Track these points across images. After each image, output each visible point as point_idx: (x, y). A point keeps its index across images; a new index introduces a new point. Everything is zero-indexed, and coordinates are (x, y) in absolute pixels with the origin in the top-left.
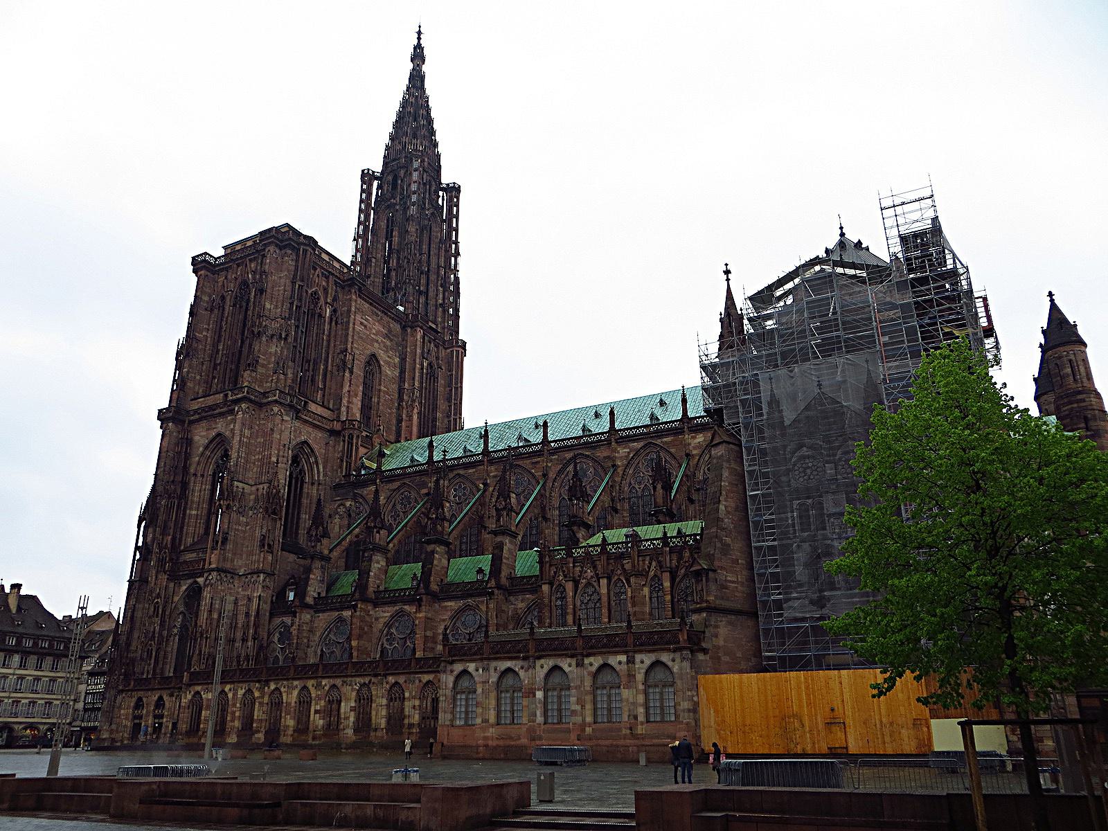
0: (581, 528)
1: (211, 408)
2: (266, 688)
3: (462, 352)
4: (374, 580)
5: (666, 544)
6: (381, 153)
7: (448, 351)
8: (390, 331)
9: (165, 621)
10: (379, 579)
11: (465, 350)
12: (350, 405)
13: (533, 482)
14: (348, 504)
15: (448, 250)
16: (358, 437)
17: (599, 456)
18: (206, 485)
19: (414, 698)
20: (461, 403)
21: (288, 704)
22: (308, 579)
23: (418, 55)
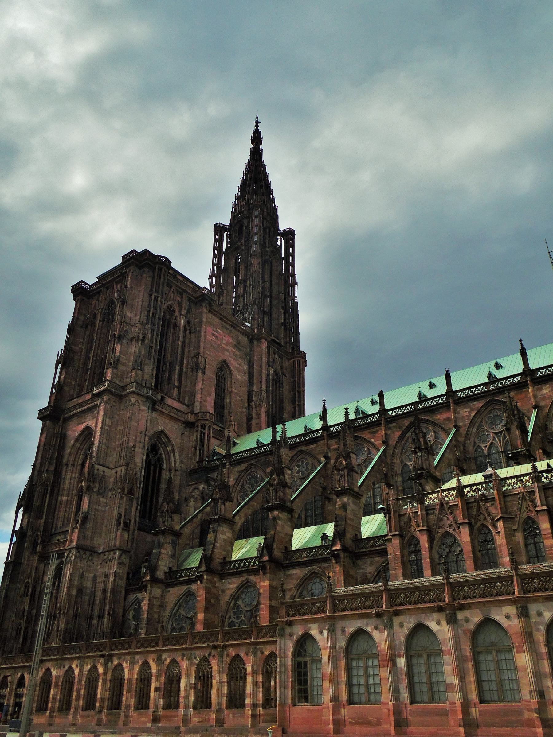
0: (429, 481)
2: (110, 663)
3: (303, 362)
4: (219, 551)
6: (230, 209)
7: (291, 361)
8: (239, 343)
9: (34, 601)
10: (224, 550)
11: (306, 361)
12: (204, 403)
14: (201, 487)
15: (287, 281)
16: (210, 427)
17: (439, 419)
20: (304, 405)
21: (130, 680)
23: (257, 138)
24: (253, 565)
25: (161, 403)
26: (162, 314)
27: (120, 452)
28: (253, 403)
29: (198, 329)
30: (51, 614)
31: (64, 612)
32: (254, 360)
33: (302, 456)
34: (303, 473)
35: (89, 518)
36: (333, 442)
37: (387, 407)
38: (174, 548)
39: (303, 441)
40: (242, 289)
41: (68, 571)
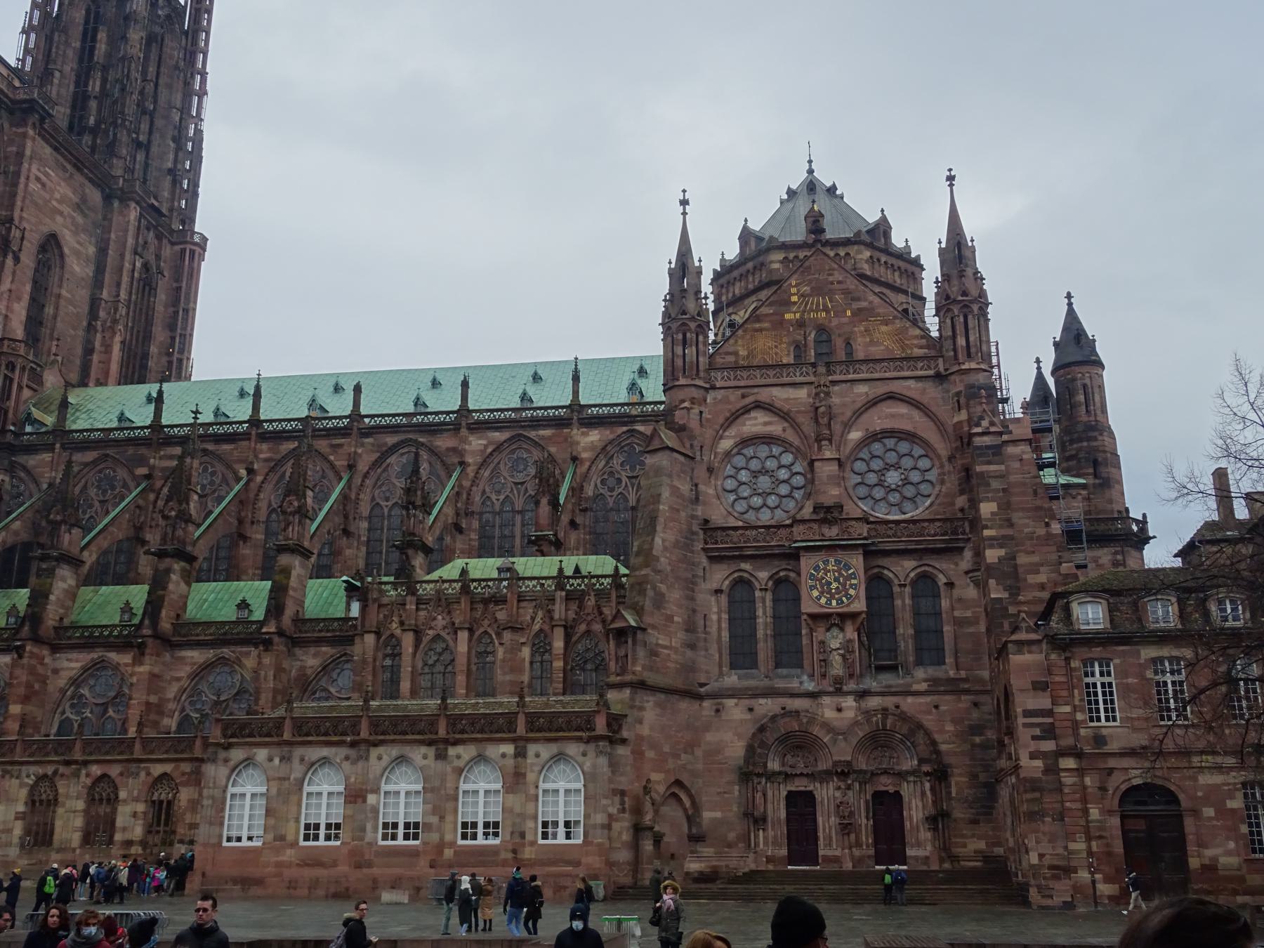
3: (200, 254)
4: (54, 607)
5: (560, 587)
7: (178, 248)
8: (84, 199)
10: (63, 606)
11: (205, 250)
13: (330, 474)
15: (188, 84)
16: (23, 369)
17: (437, 447)
19: (136, 800)
24: (116, 637)
28: (99, 323)
29: (12, 168)
32: (109, 239)
36: (264, 446)
37: (363, 411)
39: (210, 435)
40: (98, 83)
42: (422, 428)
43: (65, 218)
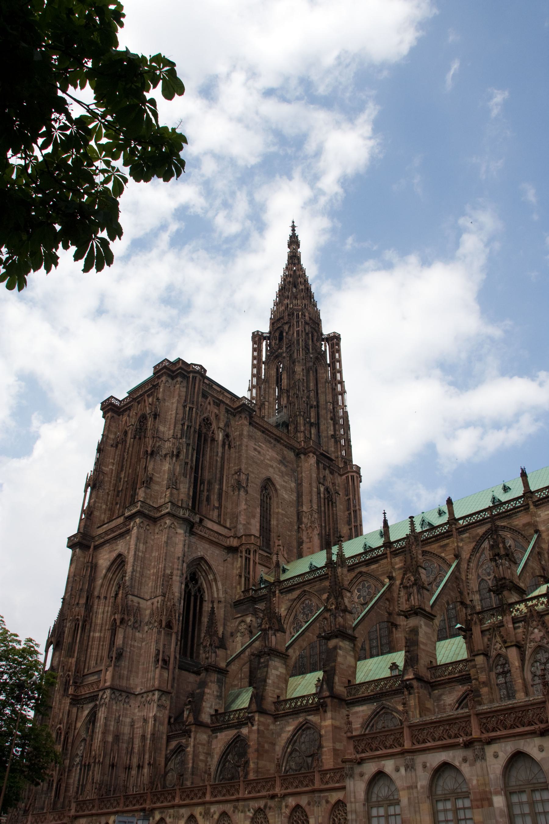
1: (112, 530)
3: (357, 477)
4: (272, 688)
7: (344, 477)
8: (284, 458)
9: (67, 749)
10: (278, 688)
11: (360, 476)
12: (249, 526)
13: (445, 567)
15: (334, 389)
16: (255, 551)
17: (517, 525)
18: (109, 606)
20: (361, 525)
22: (203, 694)
24: (312, 703)
25: (199, 526)
26: (197, 428)
27: (156, 580)
28: (303, 525)
30: (85, 763)
31: (99, 761)
32: (302, 477)
33: (363, 578)
34: (364, 597)
35: (124, 654)
36: (397, 559)
37: (457, 516)
38: (220, 687)
40: (285, 399)
41: (102, 714)
42: (501, 516)
43: (274, 469)
